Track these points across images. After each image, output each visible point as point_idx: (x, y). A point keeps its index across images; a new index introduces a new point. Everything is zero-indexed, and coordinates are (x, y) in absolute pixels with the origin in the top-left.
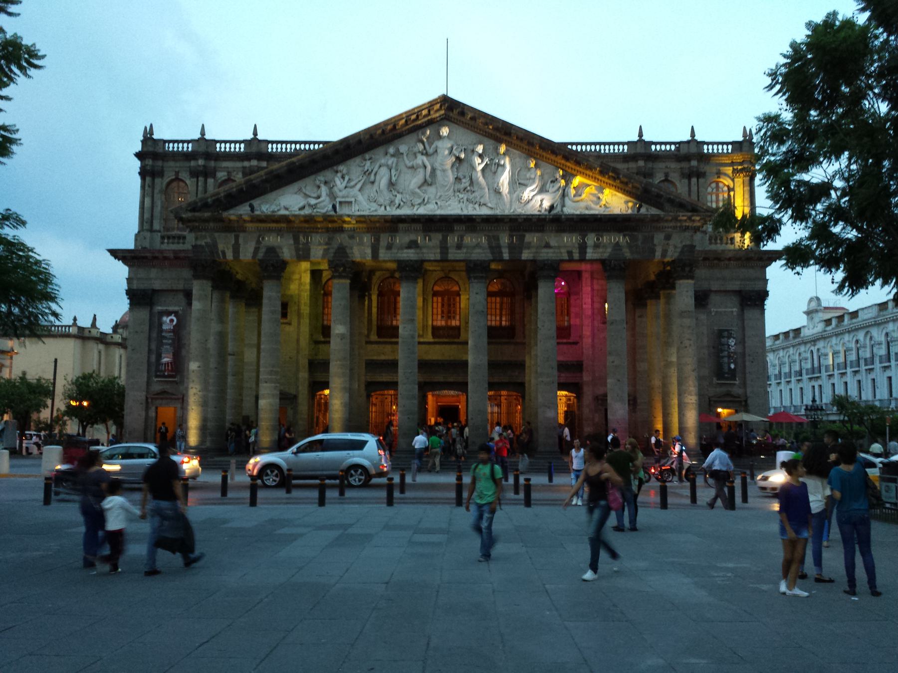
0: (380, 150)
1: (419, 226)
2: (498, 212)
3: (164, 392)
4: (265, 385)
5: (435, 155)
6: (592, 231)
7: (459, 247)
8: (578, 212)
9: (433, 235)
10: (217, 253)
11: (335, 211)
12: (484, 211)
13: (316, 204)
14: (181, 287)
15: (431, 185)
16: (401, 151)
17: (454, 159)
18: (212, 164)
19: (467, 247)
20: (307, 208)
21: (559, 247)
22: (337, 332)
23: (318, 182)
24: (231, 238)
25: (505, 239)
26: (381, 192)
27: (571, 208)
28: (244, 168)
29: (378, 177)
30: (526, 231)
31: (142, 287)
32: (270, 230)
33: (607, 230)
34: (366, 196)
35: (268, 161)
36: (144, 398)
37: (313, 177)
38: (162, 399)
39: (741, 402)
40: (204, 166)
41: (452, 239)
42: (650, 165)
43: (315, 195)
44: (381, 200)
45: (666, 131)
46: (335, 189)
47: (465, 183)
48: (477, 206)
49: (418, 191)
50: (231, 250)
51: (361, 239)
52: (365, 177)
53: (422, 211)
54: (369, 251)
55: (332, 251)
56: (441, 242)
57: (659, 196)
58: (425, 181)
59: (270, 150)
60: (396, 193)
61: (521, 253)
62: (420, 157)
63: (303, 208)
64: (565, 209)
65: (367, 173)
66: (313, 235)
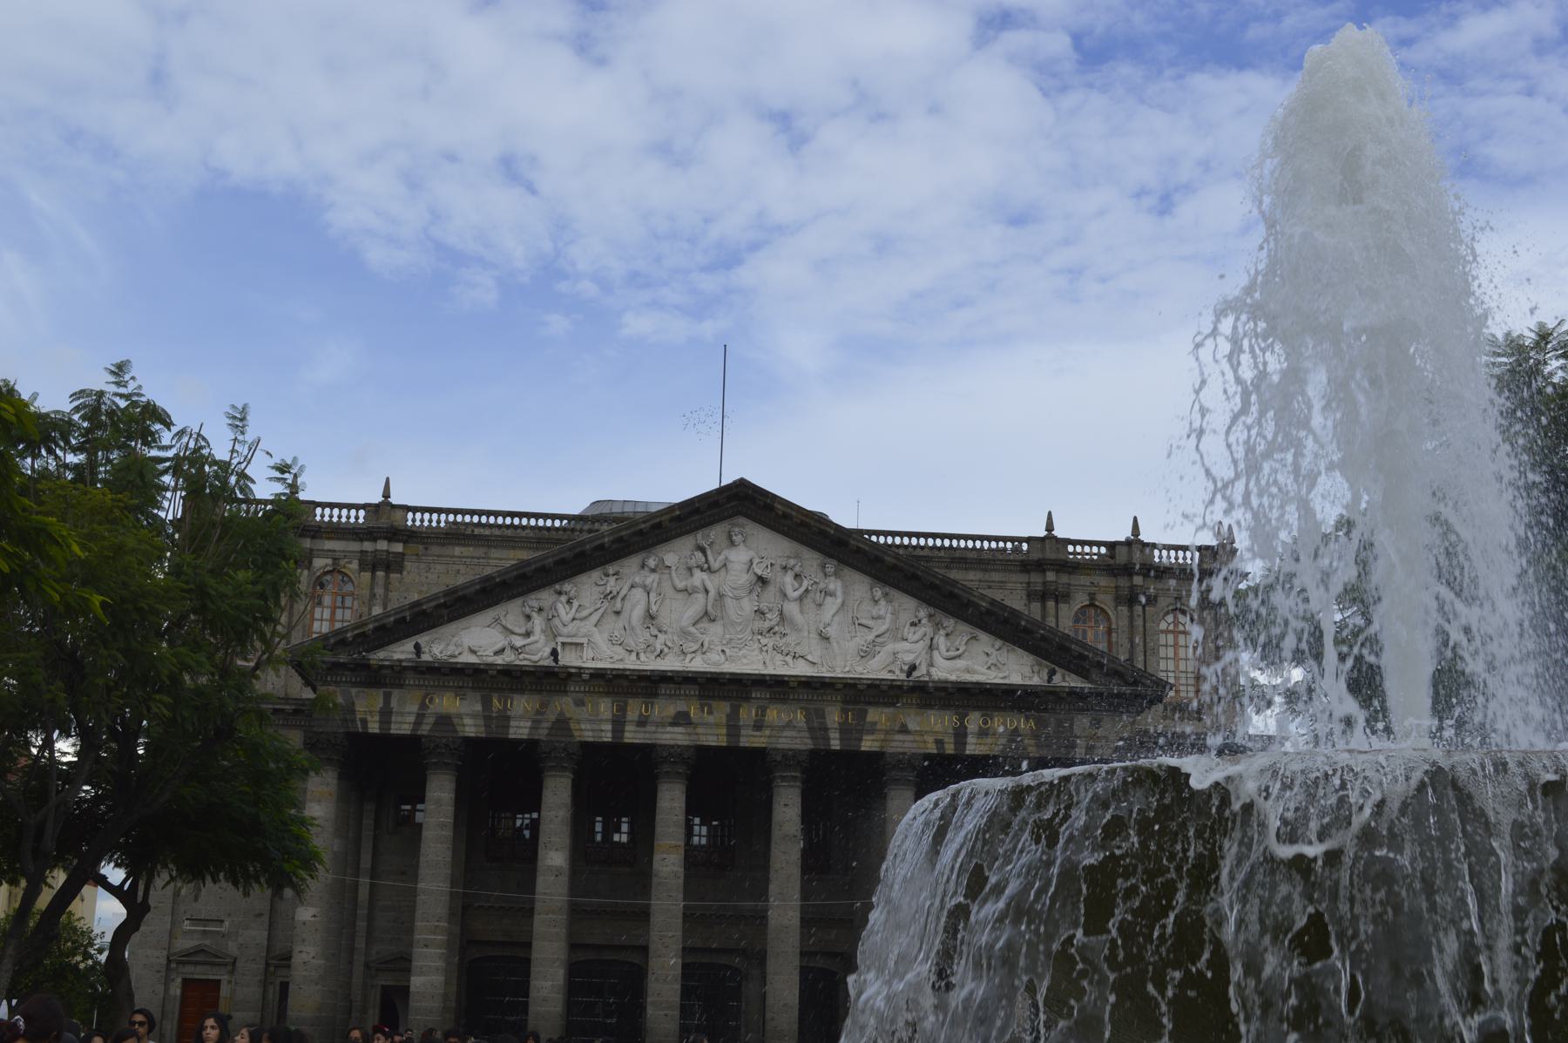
0: (632, 562)
1: (693, 690)
2: (826, 673)
3: (199, 951)
5: (723, 572)
7: (758, 726)
8: (953, 678)
9: (714, 704)
10: (354, 721)
11: (556, 660)
12: (800, 669)
19: (772, 727)
20: (508, 651)
21: (921, 733)
22: (549, 862)
23: (528, 610)
24: (376, 699)
25: (834, 716)
26: (633, 629)
27: (945, 670)
29: (628, 605)
30: (870, 703)
34: (606, 635)
35: (405, 542)
36: (164, 961)
37: (519, 601)
38: (196, 963)
41: (747, 714)
42: (1064, 579)
43: (523, 631)
44: (631, 643)
45: (1091, 522)
46: (556, 621)
47: (773, 617)
48: (789, 659)
49: (692, 629)
50: (377, 718)
52: (606, 604)
53: (697, 664)
54: (609, 727)
57: (1082, 657)
58: (706, 613)
59: (409, 523)
60: (655, 632)
61: (860, 740)
62: (697, 573)
63: (501, 651)
64: (933, 671)
65: (610, 597)
66: (516, 697)
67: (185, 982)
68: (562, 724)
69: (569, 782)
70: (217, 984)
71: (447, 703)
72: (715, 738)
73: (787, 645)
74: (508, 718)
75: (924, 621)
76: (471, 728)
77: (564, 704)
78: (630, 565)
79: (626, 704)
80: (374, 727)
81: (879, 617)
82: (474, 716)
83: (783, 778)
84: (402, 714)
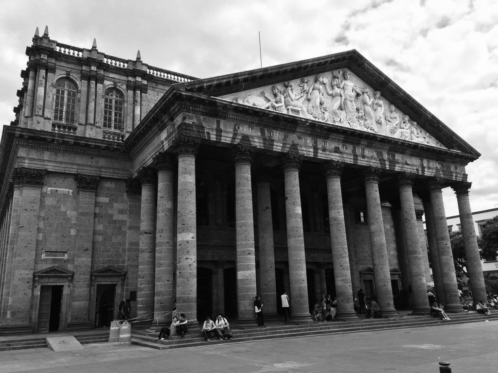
1: (342, 137)
3: (52, 270)
4: (249, 256)
6: (426, 158)
7: (364, 157)
10: (203, 133)
13: (278, 107)
14: (74, 171)
15: (342, 110)
16: (325, 82)
17: (356, 94)
18: (102, 72)
21: (413, 165)
22: (297, 212)
26: (317, 107)
28: (128, 81)
31: (33, 166)
32: (244, 122)
33: (432, 159)
35: (148, 81)
36: (31, 276)
38: (49, 277)
40: (96, 71)
41: (359, 151)
46: (288, 98)
48: (369, 129)
50: (215, 133)
51: (306, 140)
54: (312, 150)
56: (352, 151)
60: (323, 111)
61: (395, 166)
66: (274, 131)
67: (42, 287)
68: (294, 146)
69: (297, 173)
71: (245, 130)
72: (349, 160)
73: (369, 124)
74: (273, 141)
75: (407, 121)
76: (257, 143)
77: (293, 138)
78: (311, 79)
80: (213, 138)
81: (395, 118)
82: (258, 138)
83: (374, 179)
84: (226, 132)
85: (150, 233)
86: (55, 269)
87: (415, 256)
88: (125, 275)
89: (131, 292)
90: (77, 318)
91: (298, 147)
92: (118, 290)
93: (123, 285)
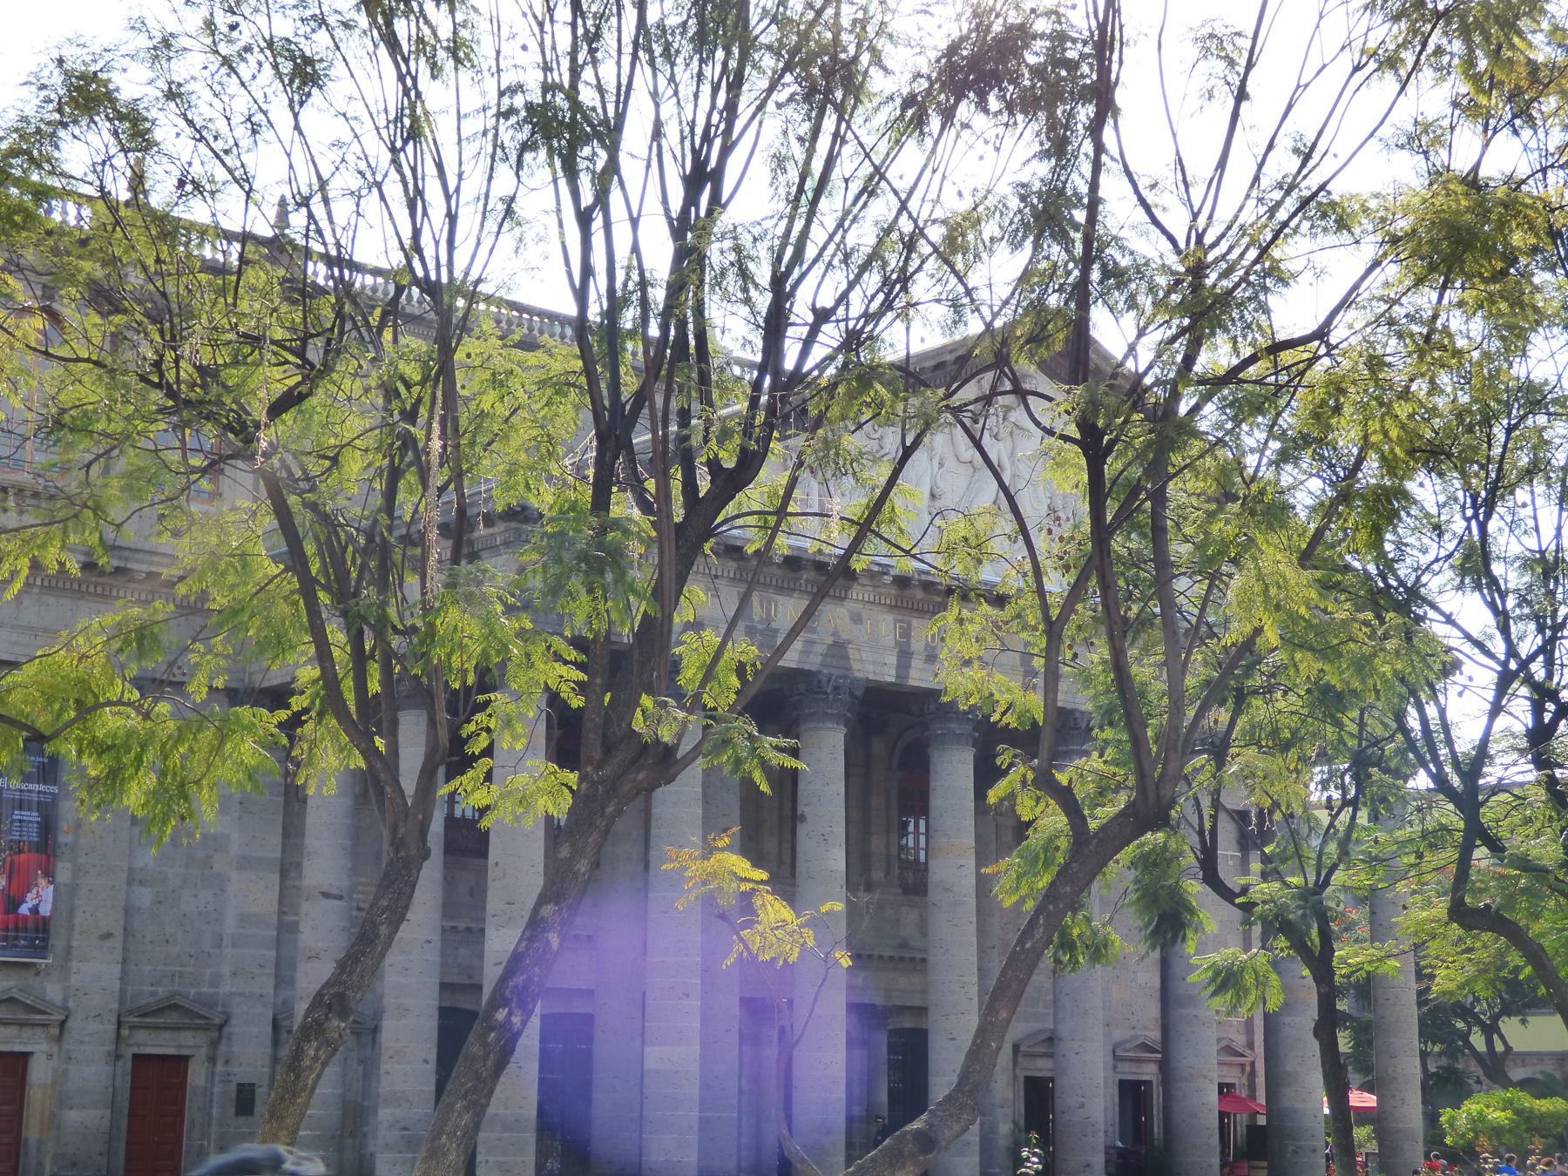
39: (1243, 1065)
54: (892, 659)
55: (820, 649)
68: (839, 649)
70: (25, 1057)
79: (909, 624)
85: (341, 898)
86: (12, 1000)
87: (1191, 1011)
88: (220, 1027)
89: (239, 1085)
90: (74, 1165)
91: (850, 651)
92: (196, 1075)
93: (212, 1060)
